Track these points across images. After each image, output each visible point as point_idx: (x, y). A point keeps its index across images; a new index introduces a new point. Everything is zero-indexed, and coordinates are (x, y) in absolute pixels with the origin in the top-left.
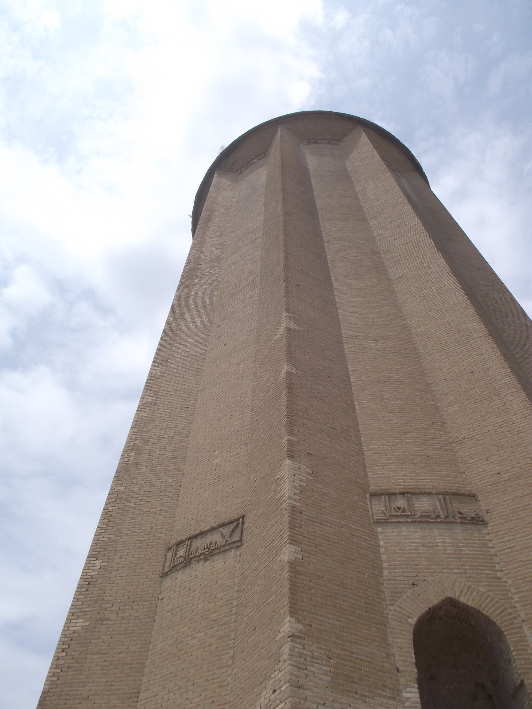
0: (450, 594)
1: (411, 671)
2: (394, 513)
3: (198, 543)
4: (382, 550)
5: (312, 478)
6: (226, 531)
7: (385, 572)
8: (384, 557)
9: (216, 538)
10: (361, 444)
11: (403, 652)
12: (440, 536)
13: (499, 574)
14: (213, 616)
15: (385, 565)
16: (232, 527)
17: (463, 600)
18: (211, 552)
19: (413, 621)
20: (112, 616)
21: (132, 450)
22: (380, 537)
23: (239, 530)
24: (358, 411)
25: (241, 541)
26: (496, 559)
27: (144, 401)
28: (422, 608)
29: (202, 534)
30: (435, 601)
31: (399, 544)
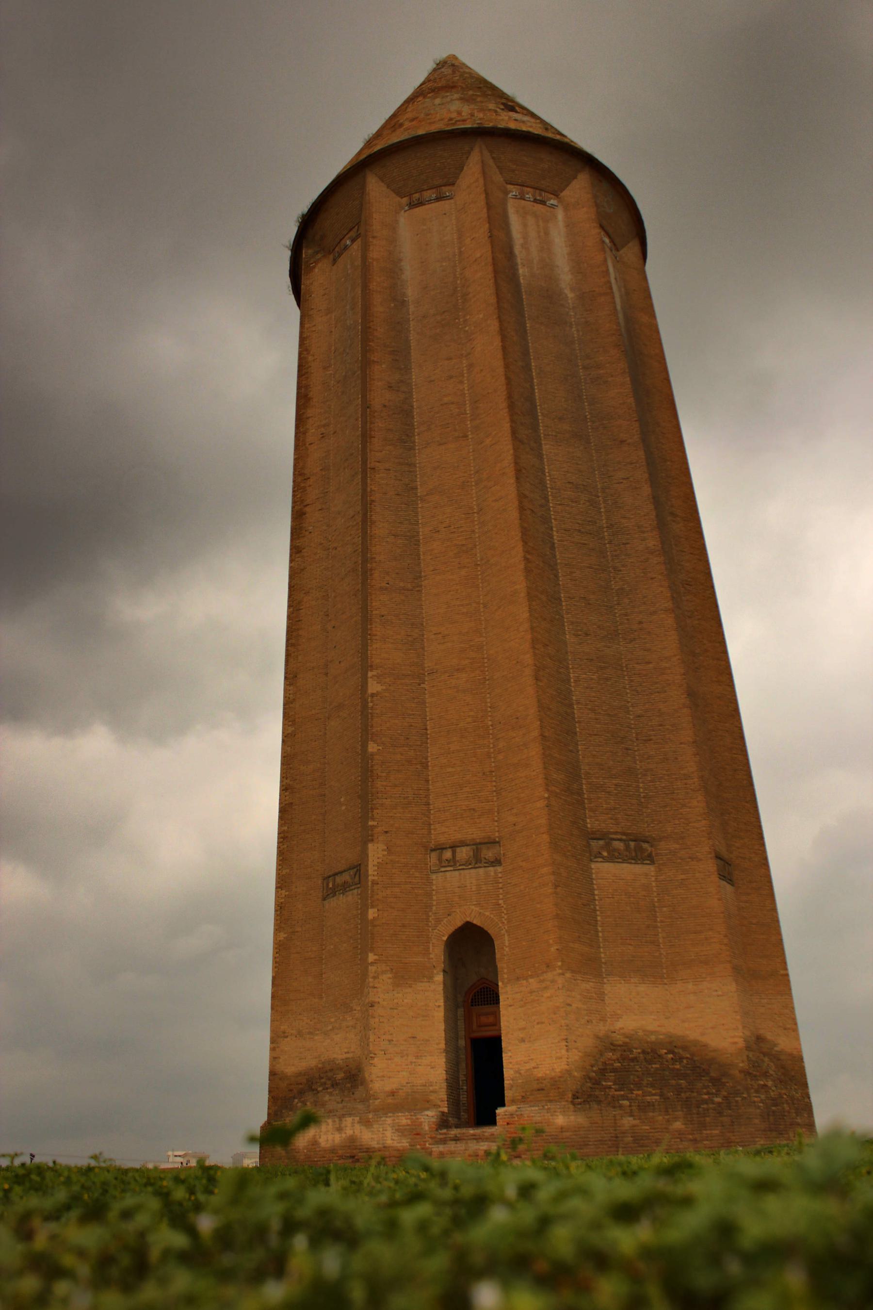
0: (468, 919)
2: (444, 864)
3: (339, 880)
4: (434, 893)
6: (352, 872)
7: (434, 908)
8: (434, 898)
9: (346, 877)
10: (429, 804)
12: (472, 877)
13: (501, 902)
15: (435, 903)
17: (475, 922)
18: (345, 888)
19: (445, 938)
20: (299, 929)
22: (434, 882)
23: (357, 876)
24: (430, 768)
26: (501, 891)
28: (451, 929)
29: (341, 873)
30: (459, 924)
31: (449, 881)
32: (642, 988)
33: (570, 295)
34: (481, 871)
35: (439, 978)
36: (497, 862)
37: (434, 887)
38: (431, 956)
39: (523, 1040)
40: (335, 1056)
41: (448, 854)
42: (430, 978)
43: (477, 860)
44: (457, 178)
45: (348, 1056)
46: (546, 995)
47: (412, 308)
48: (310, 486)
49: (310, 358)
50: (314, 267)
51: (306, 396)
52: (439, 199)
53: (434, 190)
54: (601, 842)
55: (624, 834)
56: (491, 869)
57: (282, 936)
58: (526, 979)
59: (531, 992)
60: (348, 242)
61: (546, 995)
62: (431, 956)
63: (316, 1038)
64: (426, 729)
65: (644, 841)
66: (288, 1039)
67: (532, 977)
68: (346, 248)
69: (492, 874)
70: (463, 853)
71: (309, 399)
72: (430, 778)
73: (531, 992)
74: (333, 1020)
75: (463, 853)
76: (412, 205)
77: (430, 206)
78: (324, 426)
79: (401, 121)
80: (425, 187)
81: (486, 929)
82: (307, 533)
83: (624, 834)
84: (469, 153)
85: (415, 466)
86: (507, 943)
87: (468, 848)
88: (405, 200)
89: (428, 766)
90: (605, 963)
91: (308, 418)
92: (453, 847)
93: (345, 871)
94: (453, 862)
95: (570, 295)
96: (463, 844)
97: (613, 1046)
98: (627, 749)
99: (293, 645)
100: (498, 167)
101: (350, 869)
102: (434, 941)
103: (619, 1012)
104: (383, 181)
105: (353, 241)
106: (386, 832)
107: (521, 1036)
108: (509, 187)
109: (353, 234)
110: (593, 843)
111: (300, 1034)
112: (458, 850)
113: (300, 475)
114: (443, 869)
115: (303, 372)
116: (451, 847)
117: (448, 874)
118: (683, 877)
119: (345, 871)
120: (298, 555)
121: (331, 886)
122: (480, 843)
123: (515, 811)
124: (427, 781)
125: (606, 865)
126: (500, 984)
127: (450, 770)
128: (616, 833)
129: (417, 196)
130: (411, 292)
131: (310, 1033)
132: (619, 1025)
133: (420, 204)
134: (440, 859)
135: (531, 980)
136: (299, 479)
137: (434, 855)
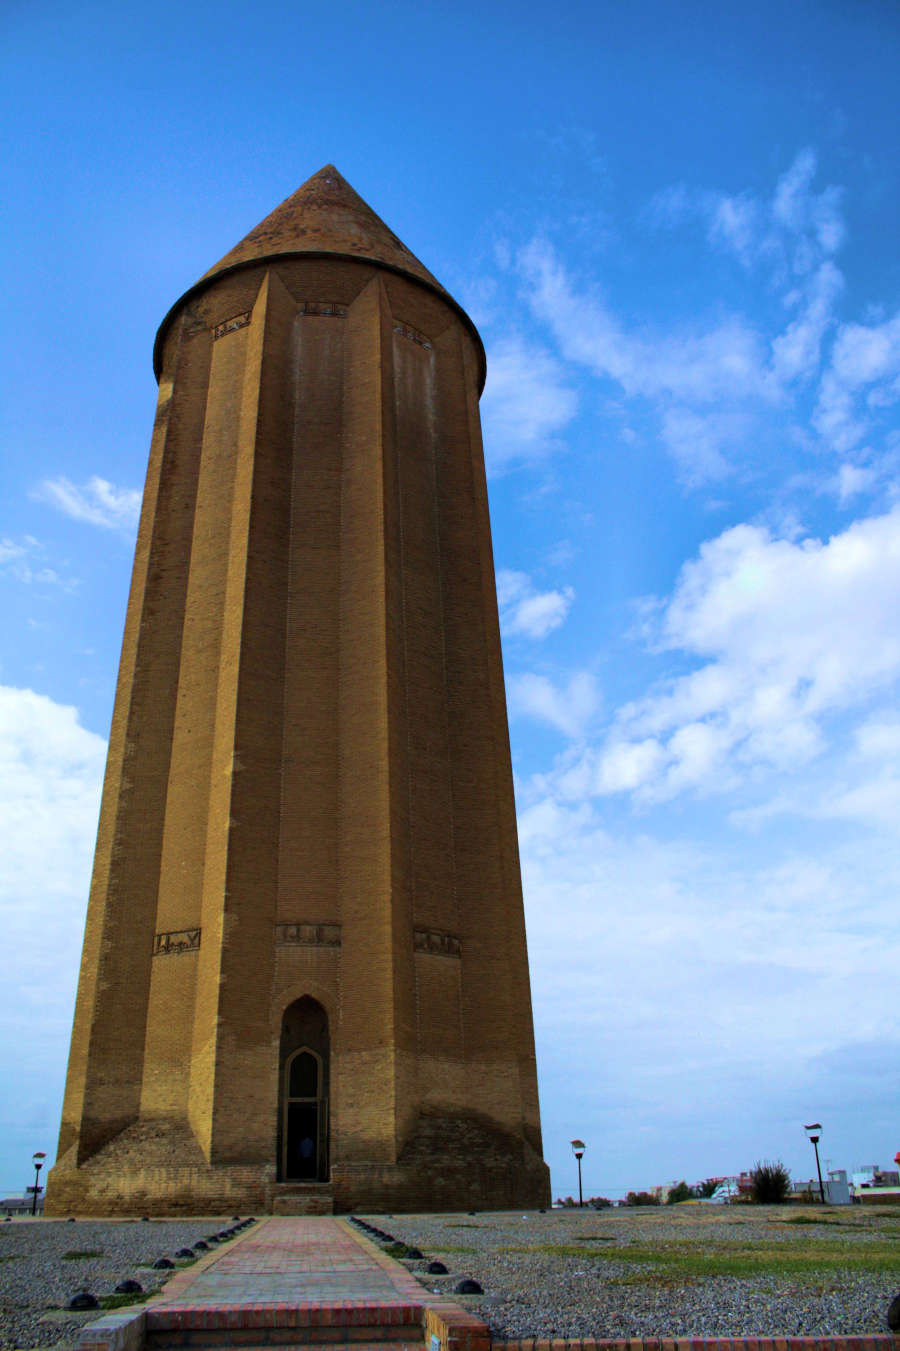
0: (307, 992)
1: (278, 1032)
5: (237, 923)
7: (276, 978)
8: (276, 969)
9: (184, 938)
11: (276, 1021)
13: (338, 979)
14: (184, 993)
16: (195, 933)
17: (313, 995)
19: (284, 1007)
20: (124, 981)
21: (120, 844)
22: (277, 955)
25: (199, 945)
27: (124, 788)
28: (290, 999)
29: (176, 932)
30: (299, 995)
32: (446, 1066)
33: (434, 435)
34: (322, 949)
35: (276, 1043)
36: (337, 943)
37: (277, 960)
38: (270, 1022)
39: (351, 1105)
40: (158, 1106)
41: (293, 930)
42: (268, 1043)
43: (319, 938)
44: (353, 301)
45: (175, 1107)
46: (378, 1067)
47: (297, 411)
48: (169, 552)
49: (180, 426)
50: (193, 337)
51: (173, 462)
52: (334, 314)
53: (330, 305)
54: (424, 935)
55: (442, 930)
56: (332, 949)
57: (105, 986)
58: (359, 1051)
59: (363, 1063)
60: (235, 326)
61: (378, 1067)
62: (270, 1022)
63: (135, 1087)
64: (279, 812)
65: (456, 938)
66: (105, 1086)
67: (364, 1050)
68: (232, 330)
69: (332, 953)
70: (307, 930)
71: (176, 466)
72: (280, 858)
73: (363, 1063)
74: (157, 1072)
75: (308, 931)
76: (307, 312)
77: (324, 318)
78: (189, 496)
79: (301, 227)
80: (322, 300)
81: (322, 1003)
82: (162, 598)
83: (442, 930)
84: (368, 281)
85: (287, 563)
86: (341, 1017)
87: (312, 927)
88: (301, 306)
89: (278, 847)
90: (420, 1042)
91: (173, 485)
92: (298, 925)
93: (182, 932)
94: (298, 937)
95: (434, 435)
96: (307, 923)
97: (422, 1115)
98: (447, 855)
99: (138, 704)
100: (390, 302)
101: (189, 930)
102: (274, 1009)
103: (428, 1085)
104: (283, 281)
105: (241, 326)
106: (239, 904)
107: (350, 1101)
108: (396, 322)
109: (242, 319)
110: (418, 935)
111: (118, 1082)
112: (303, 927)
113: (160, 538)
114: (287, 944)
115: (172, 437)
116: (295, 925)
117: (291, 949)
118: (484, 972)
119: (182, 932)
120: (150, 617)
121: (163, 943)
122: (324, 925)
123: (359, 899)
124: (277, 860)
125: (426, 956)
126: (332, 1053)
127: (299, 853)
128: (435, 928)
129: (313, 305)
130: (299, 396)
131: (128, 1082)
132: (429, 1096)
133: (315, 313)
134: (285, 935)
135: (364, 1053)
136: (158, 543)
137: (279, 929)
